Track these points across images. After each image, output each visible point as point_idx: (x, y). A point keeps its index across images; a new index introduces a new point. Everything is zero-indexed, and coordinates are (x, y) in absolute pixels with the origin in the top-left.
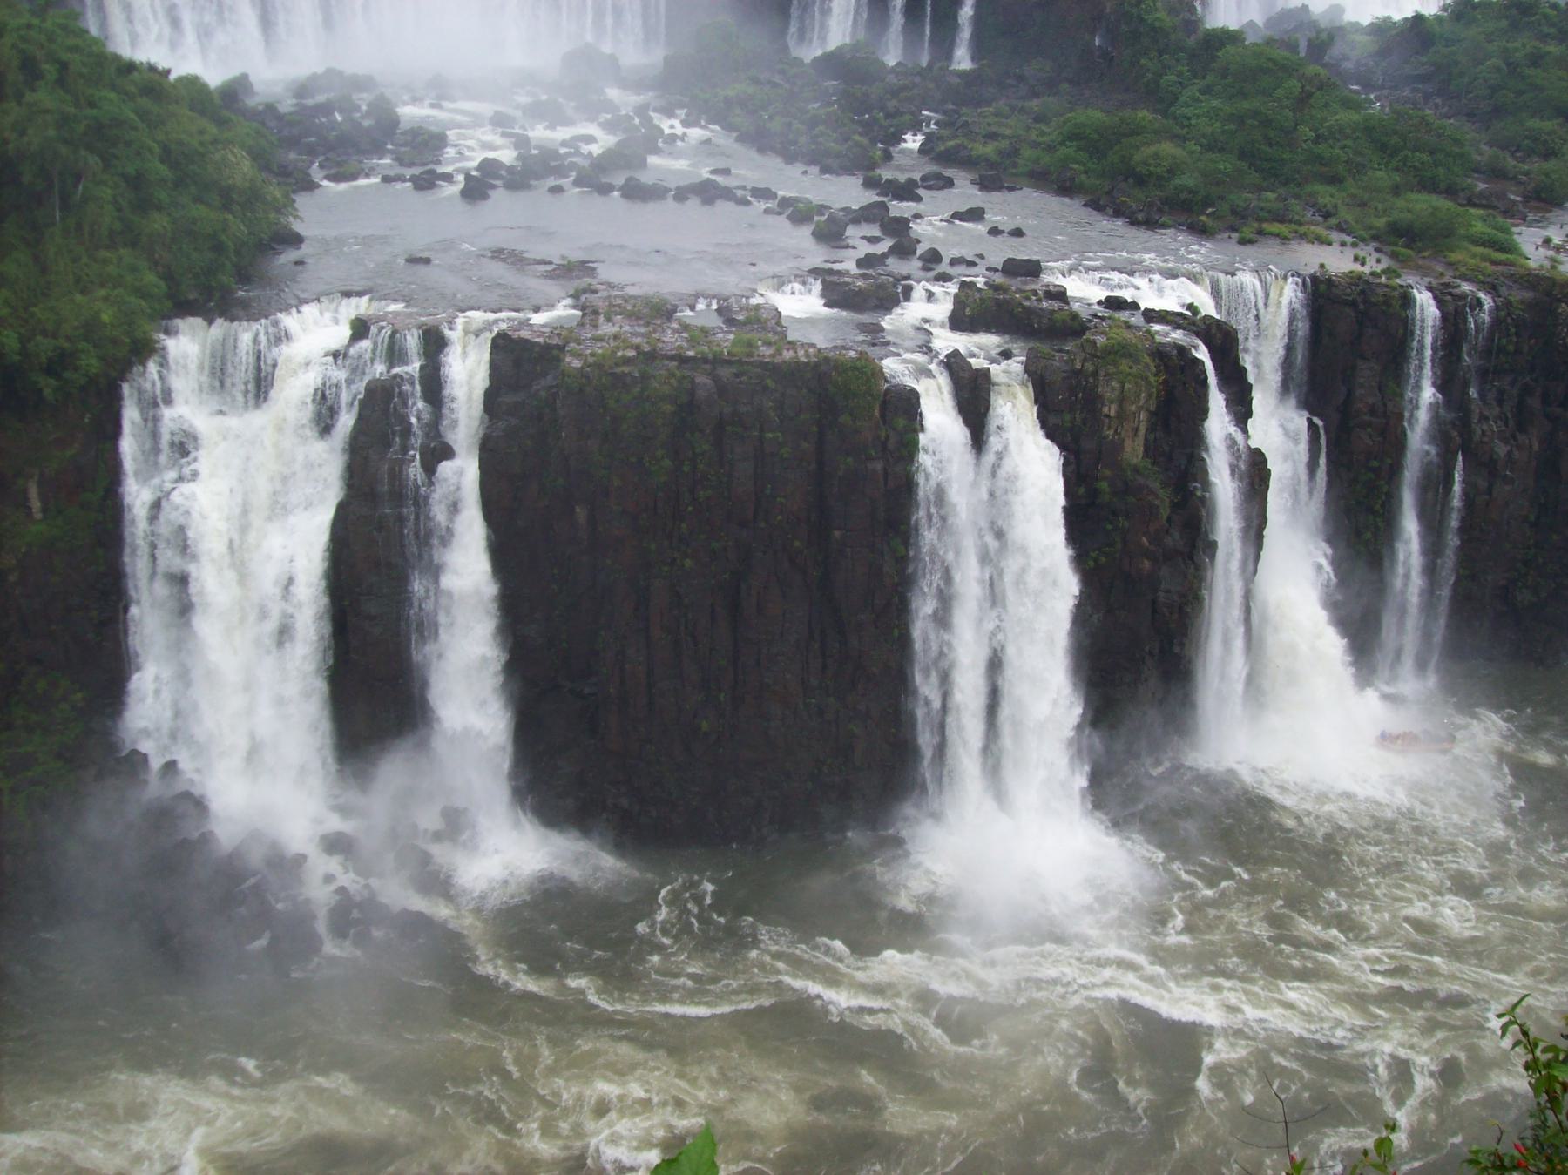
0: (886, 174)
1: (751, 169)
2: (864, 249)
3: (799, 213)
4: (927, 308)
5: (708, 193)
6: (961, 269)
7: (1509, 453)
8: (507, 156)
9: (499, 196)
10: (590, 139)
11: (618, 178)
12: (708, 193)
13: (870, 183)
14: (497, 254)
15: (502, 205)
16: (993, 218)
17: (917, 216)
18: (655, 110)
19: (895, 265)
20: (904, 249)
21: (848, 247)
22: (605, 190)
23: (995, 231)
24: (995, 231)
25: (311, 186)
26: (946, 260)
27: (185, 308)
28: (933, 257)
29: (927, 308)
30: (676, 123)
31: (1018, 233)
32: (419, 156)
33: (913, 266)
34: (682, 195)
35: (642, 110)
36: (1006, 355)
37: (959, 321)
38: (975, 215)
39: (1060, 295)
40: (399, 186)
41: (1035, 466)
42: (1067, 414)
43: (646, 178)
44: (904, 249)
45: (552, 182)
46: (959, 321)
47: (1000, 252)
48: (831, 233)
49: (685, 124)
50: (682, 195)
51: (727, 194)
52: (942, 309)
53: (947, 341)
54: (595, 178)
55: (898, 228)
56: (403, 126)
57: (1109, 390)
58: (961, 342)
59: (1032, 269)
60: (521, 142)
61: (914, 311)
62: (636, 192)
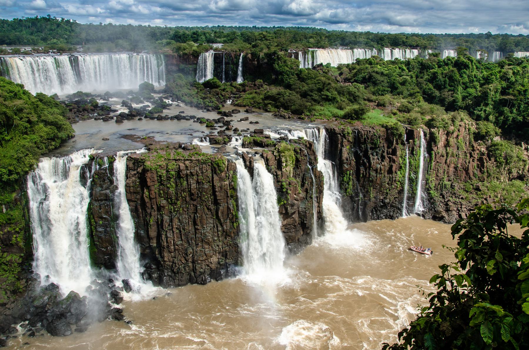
0: (223, 110)
2: (219, 129)
4: (236, 143)
5: (178, 118)
6: (244, 132)
7: (380, 168)
8: (126, 111)
10: (149, 106)
12: (178, 118)
13: (219, 113)
14: (125, 137)
15: (127, 125)
17: (231, 121)
18: (164, 98)
19: (227, 132)
21: (215, 129)
22: (152, 118)
23: (251, 123)
24: (251, 123)
26: (240, 131)
27: (44, 155)
28: (236, 130)
30: (170, 101)
31: (257, 123)
32: (103, 112)
33: (231, 133)
34: (172, 118)
35: (161, 99)
37: (243, 145)
38: (247, 119)
40: (99, 121)
41: (267, 179)
45: (138, 117)
46: (243, 145)
47: (252, 128)
49: (172, 101)
50: (172, 118)
51: (184, 118)
52: (240, 142)
53: (241, 150)
54: (150, 116)
56: (99, 105)
58: (245, 150)
59: (261, 132)
60: (130, 108)
62: (160, 119)
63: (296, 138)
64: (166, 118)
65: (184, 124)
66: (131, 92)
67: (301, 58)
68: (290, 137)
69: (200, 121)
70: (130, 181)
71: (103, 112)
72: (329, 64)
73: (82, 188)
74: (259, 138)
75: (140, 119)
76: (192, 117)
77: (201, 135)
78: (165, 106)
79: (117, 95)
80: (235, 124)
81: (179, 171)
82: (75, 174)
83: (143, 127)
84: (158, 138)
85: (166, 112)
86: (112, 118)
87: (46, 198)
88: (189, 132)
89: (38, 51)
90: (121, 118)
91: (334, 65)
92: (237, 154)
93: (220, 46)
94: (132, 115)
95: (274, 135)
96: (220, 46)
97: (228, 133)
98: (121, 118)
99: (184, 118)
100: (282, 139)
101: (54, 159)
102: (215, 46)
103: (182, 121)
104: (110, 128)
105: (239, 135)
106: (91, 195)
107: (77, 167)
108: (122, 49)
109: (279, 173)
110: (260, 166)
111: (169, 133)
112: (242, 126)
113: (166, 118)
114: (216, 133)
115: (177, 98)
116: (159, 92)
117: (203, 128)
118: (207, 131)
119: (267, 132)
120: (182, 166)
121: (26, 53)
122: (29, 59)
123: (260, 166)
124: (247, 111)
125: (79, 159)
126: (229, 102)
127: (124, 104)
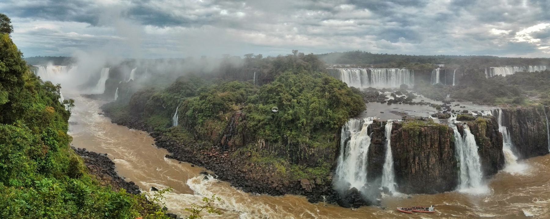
0: (445, 100)
1: (427, 100)
2: (444, 110)
3: (433, 106)
5: (421, 104)
8: (393, 99)
9: (392, 104)
11: (408, 101)
12: (421, 104)
13: (443, 102)
14: (393, 112)
15: (393, 106)
16: (461, 105)
19: (448, 112)
20: (449, 110)
22: (407, 103)
25: (367, 102)
27: (352, 117)
28: (453, 111)
29: (453, 119)
31: (464, 107)
32: (381, 99)
33: (450, 112)
34: (417, 104)
36: (465, 124)
37: (457, 120)
38: (458, 105)
39: (471, 115)
42: (474, 131)
43: (413, 102)
44: (449, 110)
46: (457, 120)
47: (462, 110)
48: (438, 108)
50: (417, 104)
51: (423, 104)
52: (455, 118)
53: (456, 122)
55: (448, 107)
57: (479, 127)
58: (458, 122)
61: (452, 118)
62: (411, 104)
63: (486, 115)
64: (414, 104)
65: (425, 107)
66: (395, 89)
67: (486, 73)
68: (483, 114)
69: (433, 106)
70: (393, 135)
71: (381, 99)
72: (501, 75)
73: (368, 137)
74: (465, 115)
75: (400, 103)
76: (429, 103)
77: (433, 113)
78: (414, 97)
79: (389, 90)
80: (452, 108)
81: (421, 132)
82: (365, 129)
83: (402, 107)
84: (409, 113)
85: (414, 100)
86: (385, 102)
87: (350, 139)
88: (427, 112)
89: (353, 67)
90: (390, 102)
91: (504, 75)
92: (454, 123)
93: (443, 65)
94: (396, 101)
95: (474, 114)
96: (443, 65)
97: (448, 112)
98: (390, 102)
99: (423, 104)
100: (478, 116)
101: (355, 120)
102: (440, 65)
103: (423, 105)
104: (384, 107)
105: (455, 114)
106: (371, 140)
107: (367, 125)
108: (393, 67)
109: (478, 134)
110: (467, 130)
111: (416, 112)
112: (456, 109)
113: (414, 104)
114: (442, 112)
115: (420, 93)
116: (410, 90)
117: (435, 110)
118: (437, 112)
119: (470, 112)
120: (423, 129)
121: (348, 68)
122: (349, 70)
123: (467, 130)
124: (458, 101)
125: (368, 122)
126: (448, 96)
127: (392, 95)
